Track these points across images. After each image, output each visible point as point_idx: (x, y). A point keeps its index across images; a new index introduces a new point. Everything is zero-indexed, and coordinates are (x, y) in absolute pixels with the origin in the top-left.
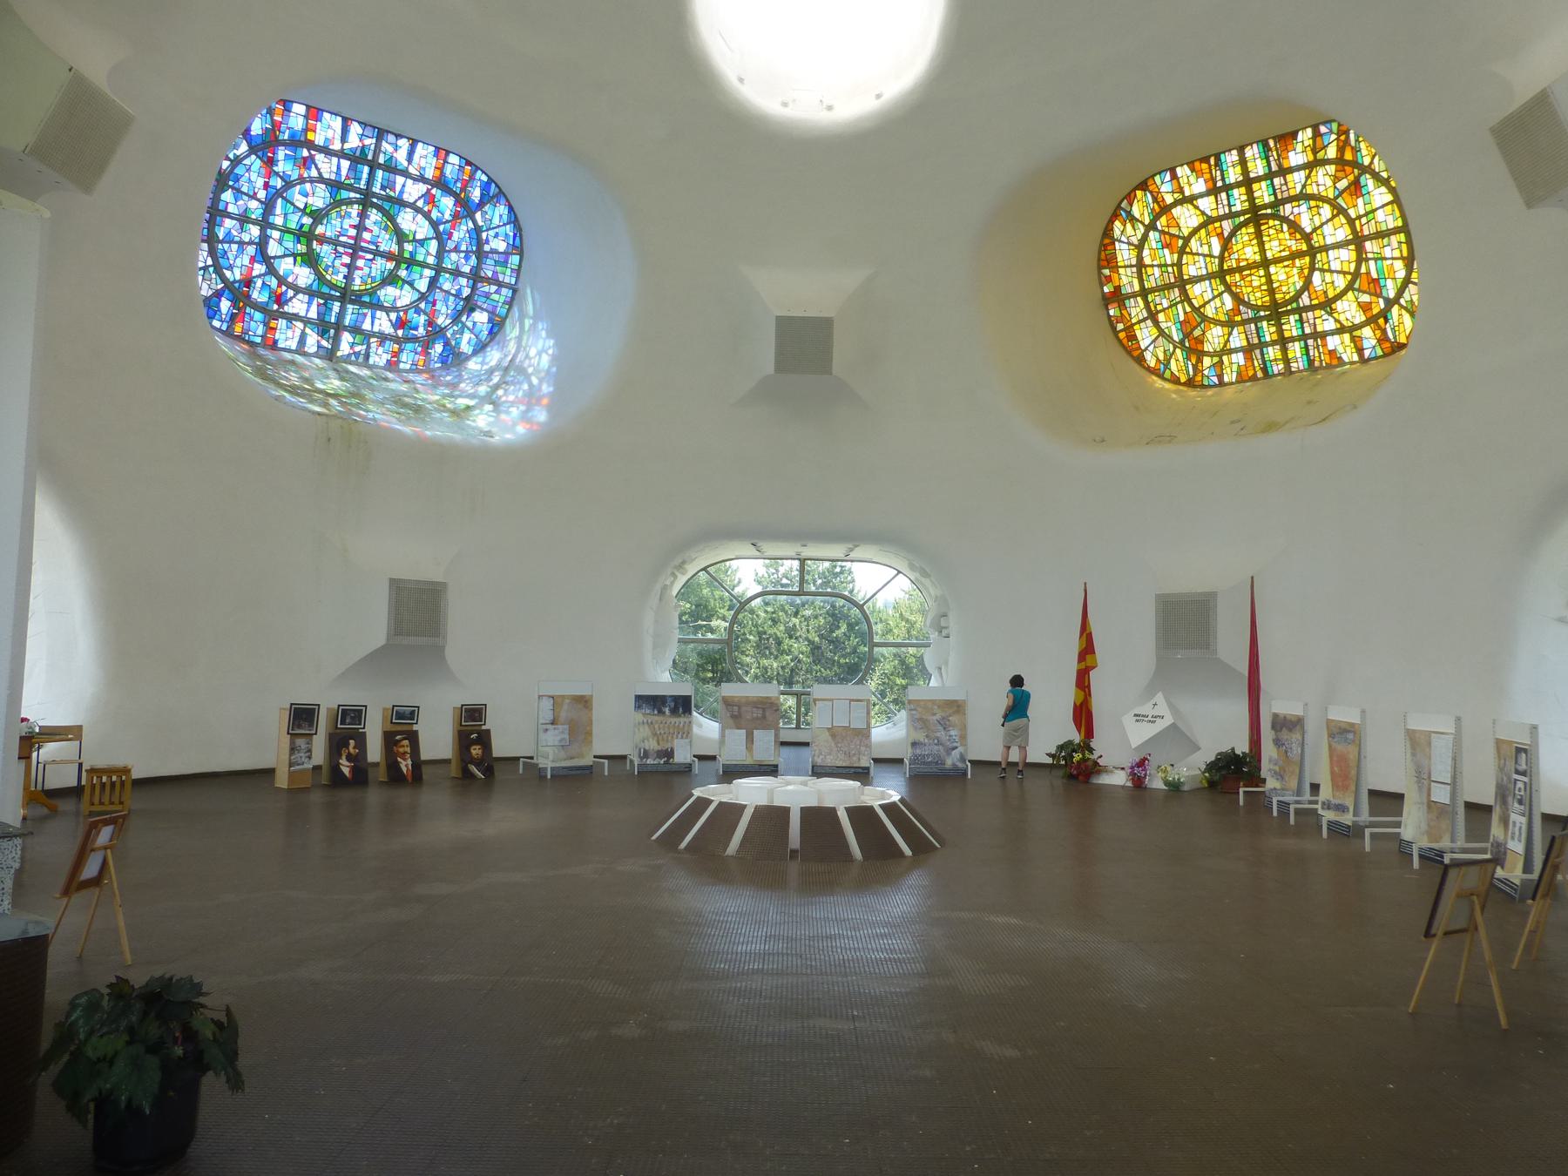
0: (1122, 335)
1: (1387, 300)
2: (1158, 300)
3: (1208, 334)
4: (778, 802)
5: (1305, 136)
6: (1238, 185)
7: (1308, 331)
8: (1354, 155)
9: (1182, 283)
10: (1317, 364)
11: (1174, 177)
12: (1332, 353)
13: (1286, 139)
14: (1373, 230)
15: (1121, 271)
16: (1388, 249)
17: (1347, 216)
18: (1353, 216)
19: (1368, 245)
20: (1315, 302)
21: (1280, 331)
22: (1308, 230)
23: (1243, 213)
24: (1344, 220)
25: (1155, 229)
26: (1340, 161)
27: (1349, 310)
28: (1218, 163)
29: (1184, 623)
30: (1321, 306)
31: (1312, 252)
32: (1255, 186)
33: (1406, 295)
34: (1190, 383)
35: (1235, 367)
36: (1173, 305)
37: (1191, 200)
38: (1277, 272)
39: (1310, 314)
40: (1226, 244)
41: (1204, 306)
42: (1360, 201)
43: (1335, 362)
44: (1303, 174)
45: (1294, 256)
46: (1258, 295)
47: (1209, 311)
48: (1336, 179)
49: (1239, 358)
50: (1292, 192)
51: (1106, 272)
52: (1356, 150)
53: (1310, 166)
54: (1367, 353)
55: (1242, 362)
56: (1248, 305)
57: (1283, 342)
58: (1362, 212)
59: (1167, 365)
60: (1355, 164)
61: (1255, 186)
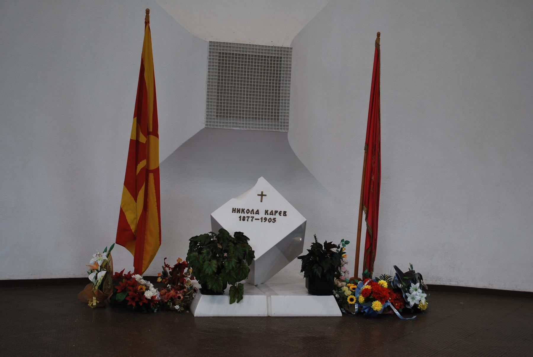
29: (251, 85)
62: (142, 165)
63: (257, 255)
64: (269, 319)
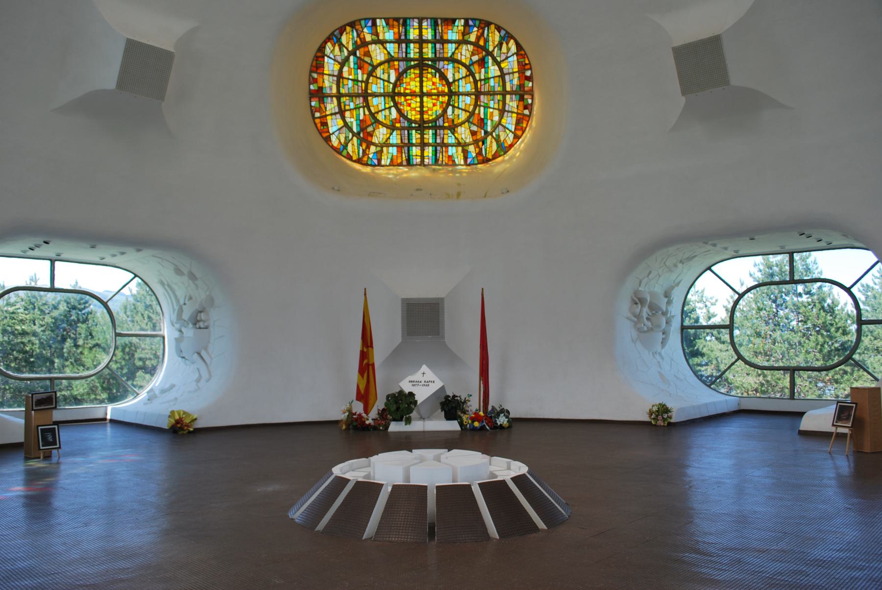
0: (317, 121)
1: (486, 132)
2: (347, 103)
3: (377, 132)
4: (416, 480)
5: (460, 23)
6: (414, 42)
7: (438, 141)
8: (485, 43)
9: (366, 95)
10: (440, 162)
11: (374, 24)
12: (450, 157)
13: (451, 22)
14: (486, 90)
15: (326, 77)
16: (492, 102)
17: (474, 78)
18: (478, 78)
19: (482, 97)
20: (446, 125)
21: (422, 138)
22: (451, 80)
23: (414, 60)
24: (472, 80)
25: (354, 54)
26: (476, 44)
27: (464, 133)
28: (405, 24)
29: (424, 319)
30: (449, 128)
31: (451, 94)
32: (424, 45)
33: (497, 131)
34: (359, 161)
35: (390, 156)
36: (357, 108)
37: (383, 43)
38: (428, 102)
39: (442, 131)
40: (400, 77)
41: (377, 113)
42: (483, 70)
43: (450, 163)
44: (454, 45)
45: (440, 94)
46: (414, 113)
47: (380, 117)
48: (473, 54)
49: (393, 150)
50: (445, 56)
51: (315, 76)
52: (486, 41)
53: (459, 43)
54: (469, 161)
55: (395, 153)
56: (406, 118)
57: (423, 145)
58: (483, 77)
59: (345, 146)
60: (484, 48)
61: (424, 45)
62: (365, 362)
63: (419, 403)
64: (424, 432)
